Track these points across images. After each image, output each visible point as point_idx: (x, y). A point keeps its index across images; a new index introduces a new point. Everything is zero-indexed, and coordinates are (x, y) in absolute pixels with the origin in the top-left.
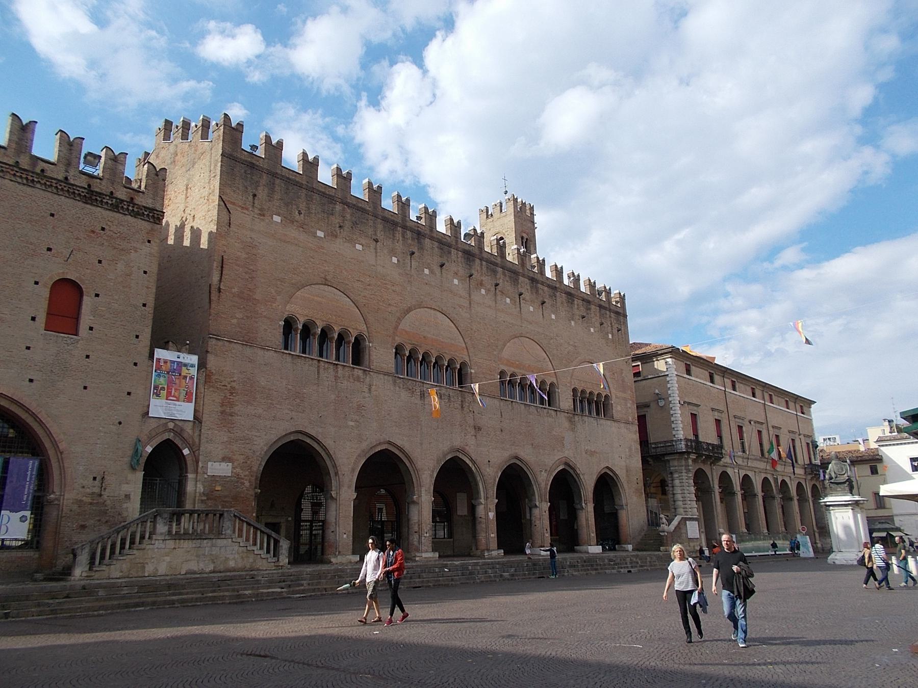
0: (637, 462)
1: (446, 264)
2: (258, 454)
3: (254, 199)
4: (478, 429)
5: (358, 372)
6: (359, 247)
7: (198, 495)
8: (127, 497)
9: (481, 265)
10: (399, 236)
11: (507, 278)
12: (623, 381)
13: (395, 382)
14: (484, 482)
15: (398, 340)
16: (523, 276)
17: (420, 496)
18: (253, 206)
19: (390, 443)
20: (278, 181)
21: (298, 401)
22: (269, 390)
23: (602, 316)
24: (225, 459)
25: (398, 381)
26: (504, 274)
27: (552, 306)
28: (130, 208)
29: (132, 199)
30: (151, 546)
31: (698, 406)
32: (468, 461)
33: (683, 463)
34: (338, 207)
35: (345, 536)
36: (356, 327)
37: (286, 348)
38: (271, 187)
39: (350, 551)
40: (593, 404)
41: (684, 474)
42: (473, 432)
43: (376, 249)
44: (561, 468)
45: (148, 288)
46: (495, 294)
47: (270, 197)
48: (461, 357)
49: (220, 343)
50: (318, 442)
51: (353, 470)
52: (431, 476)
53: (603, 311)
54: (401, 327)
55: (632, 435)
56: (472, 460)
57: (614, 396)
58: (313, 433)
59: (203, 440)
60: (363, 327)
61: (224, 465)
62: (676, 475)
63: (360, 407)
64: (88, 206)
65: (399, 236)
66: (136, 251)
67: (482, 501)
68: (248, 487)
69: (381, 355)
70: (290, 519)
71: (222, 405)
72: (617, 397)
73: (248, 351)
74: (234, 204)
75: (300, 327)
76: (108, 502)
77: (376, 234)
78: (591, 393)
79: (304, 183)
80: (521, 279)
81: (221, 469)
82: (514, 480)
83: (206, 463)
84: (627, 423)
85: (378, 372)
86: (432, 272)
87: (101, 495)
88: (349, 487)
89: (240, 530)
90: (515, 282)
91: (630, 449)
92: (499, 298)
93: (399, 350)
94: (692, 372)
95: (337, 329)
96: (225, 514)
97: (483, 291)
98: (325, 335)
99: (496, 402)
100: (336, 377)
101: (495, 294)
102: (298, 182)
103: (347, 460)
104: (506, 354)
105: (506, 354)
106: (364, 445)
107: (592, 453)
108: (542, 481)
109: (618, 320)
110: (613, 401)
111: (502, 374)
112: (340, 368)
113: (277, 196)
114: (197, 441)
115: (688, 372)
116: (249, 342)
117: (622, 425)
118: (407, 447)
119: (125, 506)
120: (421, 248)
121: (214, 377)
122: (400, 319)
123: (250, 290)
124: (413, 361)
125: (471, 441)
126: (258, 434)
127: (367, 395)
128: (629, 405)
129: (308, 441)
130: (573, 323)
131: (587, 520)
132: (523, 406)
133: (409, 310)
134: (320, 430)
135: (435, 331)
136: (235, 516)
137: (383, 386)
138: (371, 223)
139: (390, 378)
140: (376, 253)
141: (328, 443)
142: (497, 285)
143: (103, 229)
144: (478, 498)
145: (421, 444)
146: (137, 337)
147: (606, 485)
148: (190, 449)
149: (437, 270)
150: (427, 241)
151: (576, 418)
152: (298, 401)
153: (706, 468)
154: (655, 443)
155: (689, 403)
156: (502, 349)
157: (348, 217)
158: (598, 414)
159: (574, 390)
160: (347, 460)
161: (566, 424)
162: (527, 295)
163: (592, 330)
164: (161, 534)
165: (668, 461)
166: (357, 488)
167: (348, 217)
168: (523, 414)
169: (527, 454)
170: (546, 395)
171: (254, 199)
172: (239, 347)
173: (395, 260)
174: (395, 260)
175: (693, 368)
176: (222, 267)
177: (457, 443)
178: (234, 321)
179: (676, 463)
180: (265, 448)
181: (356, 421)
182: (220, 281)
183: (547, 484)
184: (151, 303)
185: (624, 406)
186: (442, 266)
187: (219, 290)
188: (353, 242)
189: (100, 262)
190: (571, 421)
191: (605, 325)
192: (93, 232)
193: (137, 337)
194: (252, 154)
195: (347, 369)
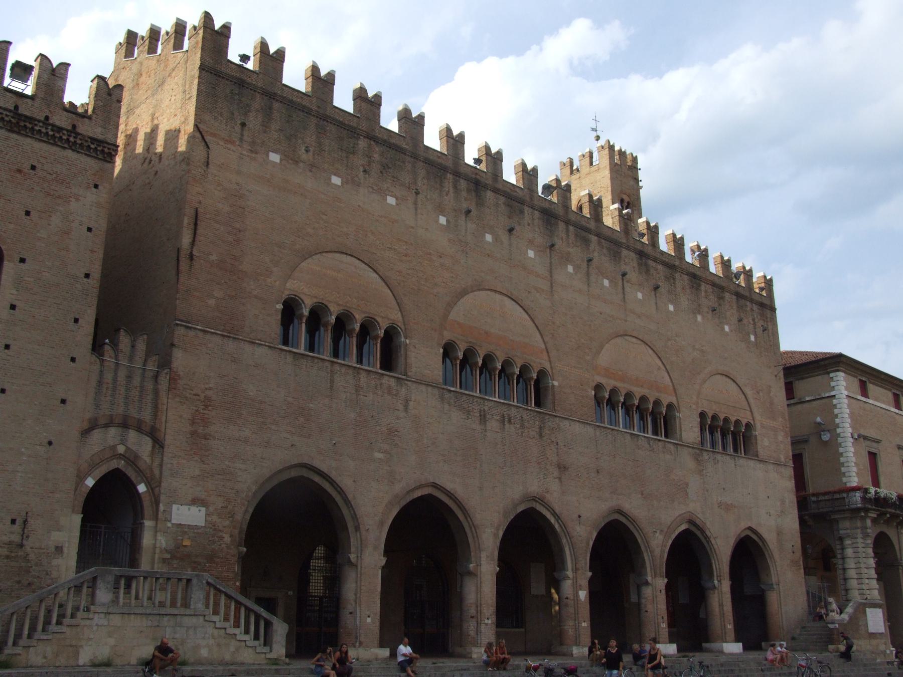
0: (791, 522)
1: (517, 228)
3: (242, 130)
4: (562, 468)
5: (388, 381)
6: (391, 200)
7: (158, 551)
8: (59, 549)
9: (567, 231)
10: (448, 184)
11: (605, 251)
12: (772, 403)
13: (442, 398)
14: (573, 546)
15: (448, 336)
16: (628, 248)
17: (479, 565)
18: (241, 140)
19: (435, 486)
20: (276, 105)
21: (302, 419)
23: (740, 308)
24: (195, 501)
25: (447, 395)
26: (599, 243)
27: (670, 292)
28: (72, 139)
29: (74, 127)
30: (88, 622)
31: (878, 441)
32: (548, 515)
33: (859, 524)
34: (362, 143)
35: (369, 620)
36: (387, 316)
37: (285, 342)
38: (268, 113)
39: (376, 642)
40: (729, 436)
41: (860, 540)
42: (556, 473)
43: (415, 203)
44: (684, 527)
45: (92, 251)
46: (588, 274)
47: (265, 126)
48: (539, 362)
49: (192, 333)
50: (332, 482)
51: (382, 523)
52: (495, 535)
53: (742, 302)
54: (452, 316)
55: (785, 483)
56: (554, 514)
57: (758, 426)
58: (323, 468)
59: (166, 473)
60: (396, 316)
61: (194, 509)
62: (848, 542)
63: (392, 432)
64: (14, 136)
65: (448, 184)
66: (77, 200)
67: (569, 573)
68: (229, 542)
69: (423, 357)
70: (291, 593)
71: (193, 422)
72: (763, 426)
73: (231, 345)
74: (214, 135)
75: (306, 312)
76: (32, 556)
77: (415, 183)
78: (726, 420)
79: (314, 108)
80: (625, 252)
81: (189, 515)
82: (689, 550)
84: (777, 464)
85: (419, 382)
86: (496, 239)
87: (21, 546)
88: (376, 548)
89: (216, 604)
90: (616, 256)
91: (783, 502)
92: (593, 278)
93: (448, 351)
94: (870, 393)
95: (359, 317)
96: (195, 581)
97: (570, 269)
98: (341, 325)
99: (590, 430)
100: (358, 388)
101: (588, 274)
102: (304, 107)
103: (372, 508)
104: (604, 359)
105: (604, 359)
106: (398, 488)
107: (728, 507)
108: (657, 546)
109: (762, 315)
111: (598, 387)
112: (363, 375)
113: (274, 126)
114: (157, 472)
115: (865, 393)
116: (231, 333)
117: (771, 467)
118: (459, 491)
119: (55, 562)
120: (480, 203)
122: (450, 305)
124: (468, 365)
125: (554, 486)
127: (402, 414)
128: (780, 438)
129: (317, 479)
130: (699, 318)
131: (721, 605)
132: (628, 437)
133: (464, 293)
135: (501, 324)
136: (208, 583)
137: (424, 402)
138: (409, 166)
139: (436, 391)
140: (416, 209)
141: (346, 483)
142: (590, 260)
143: (33, 168)
144: (563, 568)
145: (481, 488)
146: (76, 321)
147: (749, 553)
148: (148, 484)
149: (504, 237)
150: (489, 194)
151: (705, 455)
153: (891, 533)
154: (813, 495)
155: (866, 438)
156: (598, 352)
157: (376, 156)
158: (736, 450)
159: (702, 415)
160: (372, 508)
161: (691, 463)
162: (633, 276)
163: (727, 328)
164: (104, 605)
165: (837, 521)
166: (387, 552)
167: (376, 156)
169: (634, 506)
170: (658, 420)
171: (242, 130)
172: (218, 339)
173: (443, 220)
174: (443, 220)
175: (871, 387)
176: (196, 224)
177: (534, 488)
178: (212, 302)
179: (847, 524)
180: (254, 488)
181: (385, 452)
182: (193, 243)
183: (662, 551)
184: (96, 274)
185: (772, 439)
186: (511, 230)
187: (191, 257)
188: (383, 193)
189: (28, 213)
190: (698, 460)
191: (745, 321)
192: (19, 171)
193: (76, 321)
194: (241, 66)
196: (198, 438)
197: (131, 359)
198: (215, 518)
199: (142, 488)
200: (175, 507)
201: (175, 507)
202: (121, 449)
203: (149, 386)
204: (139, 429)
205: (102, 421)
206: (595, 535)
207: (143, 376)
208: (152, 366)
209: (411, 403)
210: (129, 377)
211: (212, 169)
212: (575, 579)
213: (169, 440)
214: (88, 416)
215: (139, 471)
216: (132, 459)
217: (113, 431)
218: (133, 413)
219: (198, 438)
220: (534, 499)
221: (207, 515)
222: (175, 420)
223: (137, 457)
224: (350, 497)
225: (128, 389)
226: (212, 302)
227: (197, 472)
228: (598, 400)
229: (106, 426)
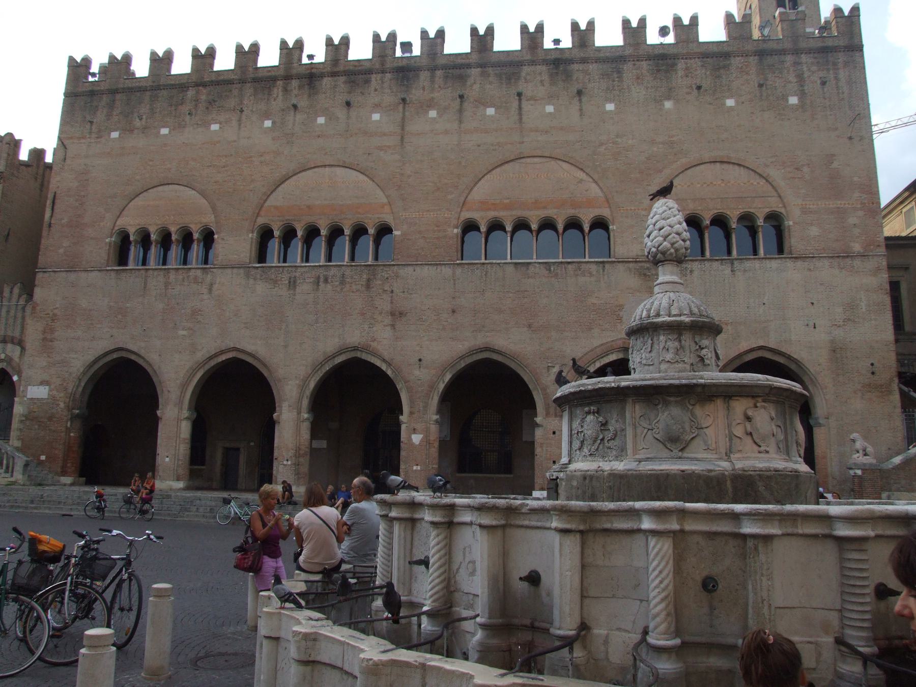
2: (74, 375)
22: (90, 310)
24: (42, 383)
49: (47, 275)
61: (42, 388)
73: (72, 276)
83: (26, 387)
85: (223, 267)
121: (38, 308)
126: (75, 356)
127: (205, 297)
134: (143, 344)
152: (120, 317)
172: (64, 274)
178: (61, 251)
195: (180, 272)
196: (47, 342)
197: (10, 300)
198: (55, 392)
200: (29, 388)
201: (29, 388)
203: (20, 315)
204: (13, 343)
207: (17, 309)
208: (22, 302)
209: (215, 287)
210: (8, 312)
213: (28, 346)
216: (9, 360)
218: (10, 333)
219: (47, 342)
221: (50, 390)
222: (33, 332)
225: (7, 319)
226: (61, 251)
227: (45, 364)
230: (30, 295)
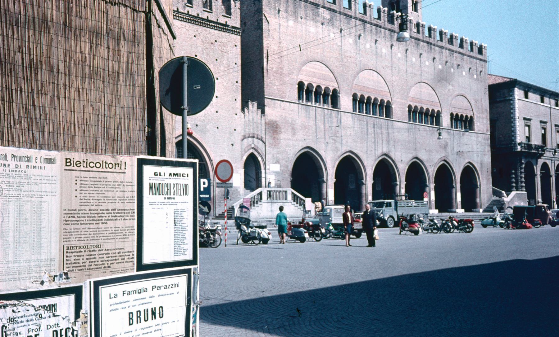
0: (488, 159)
15: (354, 92)
32: (390, 161)
36: (332, 86)
44: (442, 163)
57: (475, 117)
60: (336, 86)
105: (412, 94)
106: (339, 153)
108: (431, 171)
110: (475, 120)
111: (410, 107)
123: (281, 69)
144: (396, 181)
147: (469, 173)
148: (262, 157)
168: (425, 131)
169: (423, 156)
199: (260, 159)
202: (253, 146)
204: (258, 138)
205: (247, 136)
206: (407, 167)
211: (271, 32)
212: (400, 185)
214: (242, 134)
215: (259, 153)
217: (250, 139)
220: (386, 155)
223: (258, 147)
224: (323, 158)
228: (409, 111)
229: (248, 137)
230: (263, 112)
